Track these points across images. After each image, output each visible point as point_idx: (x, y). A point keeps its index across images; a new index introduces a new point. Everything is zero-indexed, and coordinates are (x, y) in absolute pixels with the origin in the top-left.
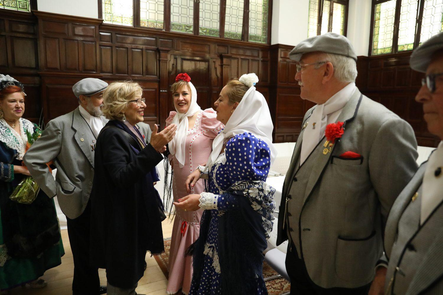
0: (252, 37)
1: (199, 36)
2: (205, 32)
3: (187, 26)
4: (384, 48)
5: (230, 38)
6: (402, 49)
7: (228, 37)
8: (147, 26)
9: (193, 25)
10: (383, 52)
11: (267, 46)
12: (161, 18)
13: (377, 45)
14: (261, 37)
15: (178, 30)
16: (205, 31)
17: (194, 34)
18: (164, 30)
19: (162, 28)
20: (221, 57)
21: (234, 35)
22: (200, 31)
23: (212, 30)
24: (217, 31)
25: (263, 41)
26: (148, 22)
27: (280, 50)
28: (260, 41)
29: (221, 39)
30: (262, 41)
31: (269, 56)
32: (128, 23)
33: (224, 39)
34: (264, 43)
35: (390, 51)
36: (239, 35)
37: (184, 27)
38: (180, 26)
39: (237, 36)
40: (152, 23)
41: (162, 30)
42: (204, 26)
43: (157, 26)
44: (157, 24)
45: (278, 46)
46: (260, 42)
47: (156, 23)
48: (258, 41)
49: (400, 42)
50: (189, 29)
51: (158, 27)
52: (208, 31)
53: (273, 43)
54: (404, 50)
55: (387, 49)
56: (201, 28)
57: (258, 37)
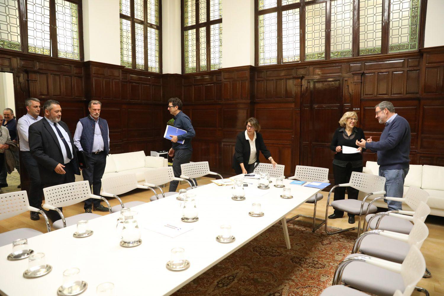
0: (392, 48)
2: (337, 55)
3: (320, 54)
5: (367, 54)
7: (365, 54)
8: (288, 61)
9: (324, 52)
12: (298, 52)
15: (312, 59)
16: (337, 54)
18: (300, 62)
19: (299, 60)
21: (371, 50)
22: (332, 55)
23: (344, 52)
24: (349, 51)
25: (411, 49)
26: (288, 58)
28: (407, 49)
32: (274, 62)
36: (378, 49)
37: (316, 55)
38: (313, 55)
39: (375, 50)
40: (291, 58)
41: (298, 61)
42: (335, 50)
43: (295, 59)
44: (295, 58)
47: (294, 57)
48: (403, 50)
50: (321, 56)
51: (296, 60)
52: (339, 53)
56: (332, 53)
57: (404, 46)
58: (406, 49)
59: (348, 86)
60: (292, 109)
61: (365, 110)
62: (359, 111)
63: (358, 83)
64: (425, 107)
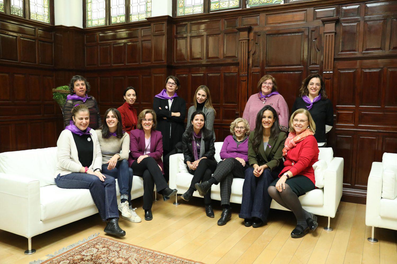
4: (98, 20)
49: (114, 12)
54: (117, 22)
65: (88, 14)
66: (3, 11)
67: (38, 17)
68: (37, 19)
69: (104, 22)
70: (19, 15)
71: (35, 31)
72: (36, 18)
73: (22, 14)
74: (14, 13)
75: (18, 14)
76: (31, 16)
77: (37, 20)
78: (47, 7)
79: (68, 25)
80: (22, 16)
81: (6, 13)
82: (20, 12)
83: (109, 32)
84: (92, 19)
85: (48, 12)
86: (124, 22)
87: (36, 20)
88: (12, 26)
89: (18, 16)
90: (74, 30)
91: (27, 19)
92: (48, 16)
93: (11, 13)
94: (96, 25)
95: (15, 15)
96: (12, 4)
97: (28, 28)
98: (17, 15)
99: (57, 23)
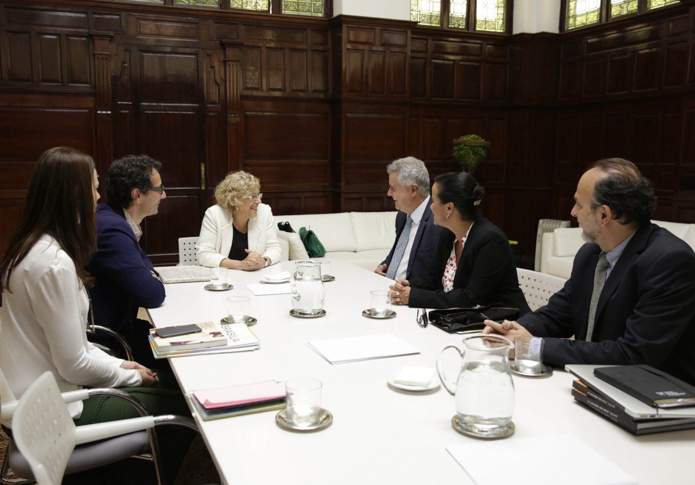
1: (174, 6)
4: (587, 14)
6: (618, 13)
10: (584, 22)
11: (326, 21)
13: (575, 8)
14: (311, 4)
17: (165, 4)
20: (223, 46)
25: (314, 12)
27: (344, 27)
28: (309, 11)
29: (222, 10)
30: (313, 11)
31: (329, 39)
33: (230, 11)
34: (320, 15)
35: (597, 18)
45: (342, 19)
46: (309, 14)
48: (304, 12)
53: (336, 14)
55: (593, 14)
57: (305, 4)
58: (307, 12)
59: (213, 67)
60: (87, 111)
61: (246, 117)
62: (239, 120)
63: (234, 63)
64: (348, 115)
65: (569, 6)
66: (439, 25)
67: (487, 25)
68: (485, 28)
69: (596, 17)
70: (461, 27)
71: (481, 47)
72: (484, 26)
73: (464, 23)
74: (454, 24)
75: (459, 25)
76: (477, 25)
77: (486, 30)
78: (503, 5)
79: (534, 30)
80: (463, 27)
81: (442, 27)
82: (461, 21)
83: (609, 33)
84: (576, 15)
85: (503, 15)
86: (635, 13)
87: (484, 30)
88: (451, 44)
89: (458, 28)
90: (543, 37)
91: (471, 31)
92: (503, 20)
93: (450, 26)
94: (583, 24)
95: (454, 28)
96: (452, 12)
97: (473, 45)
98: (456, 27)
99: (516, 30)
